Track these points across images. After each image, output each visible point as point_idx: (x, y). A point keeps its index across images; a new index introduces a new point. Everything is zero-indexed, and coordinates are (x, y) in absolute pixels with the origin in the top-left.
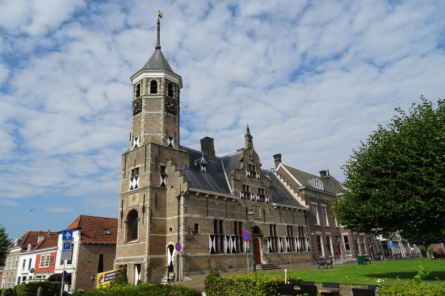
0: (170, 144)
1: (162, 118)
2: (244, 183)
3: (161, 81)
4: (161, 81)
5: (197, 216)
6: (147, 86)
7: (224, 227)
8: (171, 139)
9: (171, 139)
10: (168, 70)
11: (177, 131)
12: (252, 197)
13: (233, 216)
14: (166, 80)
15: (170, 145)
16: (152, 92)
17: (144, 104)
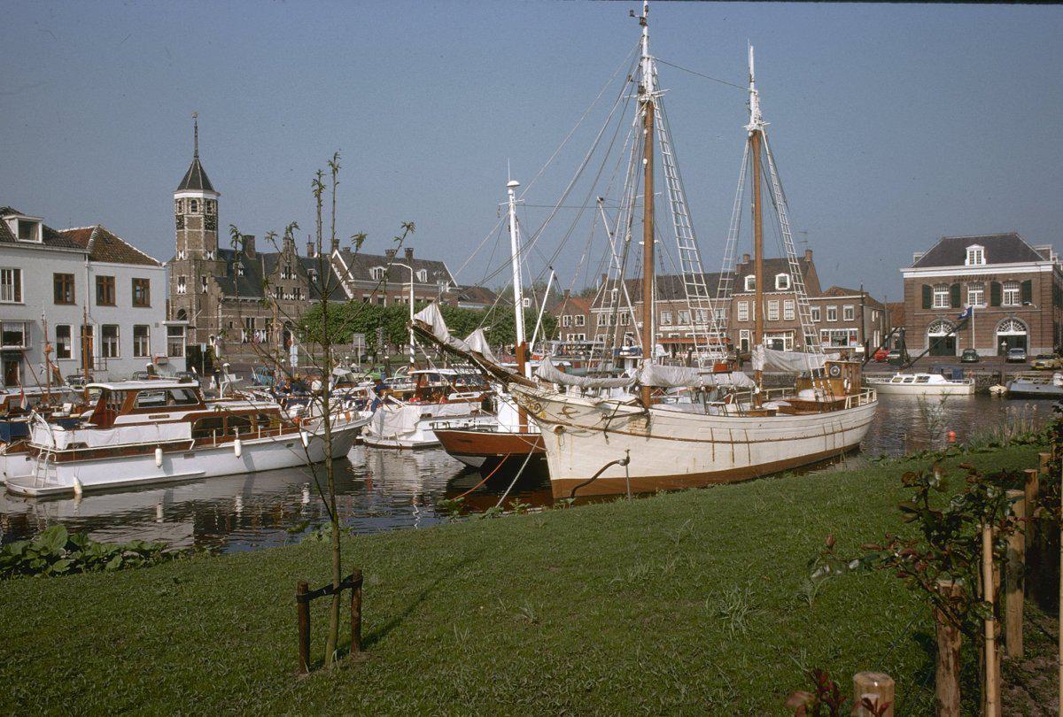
0: (210, 258)
1: (202, 235)
2: (277, 285)
3: (200, 201)
4: (200, 201)
5: (232, 316)
6: (188, 206)
7: (255, 323)
8: (210, 252)
9: (210, 252)
10: (207, 187)
11: (215, 244)
12: (285, 296)
13: (264, 314)
14: (205, 199)
15: (210, 258)
16: (193, 211)
17: (186, 223)
